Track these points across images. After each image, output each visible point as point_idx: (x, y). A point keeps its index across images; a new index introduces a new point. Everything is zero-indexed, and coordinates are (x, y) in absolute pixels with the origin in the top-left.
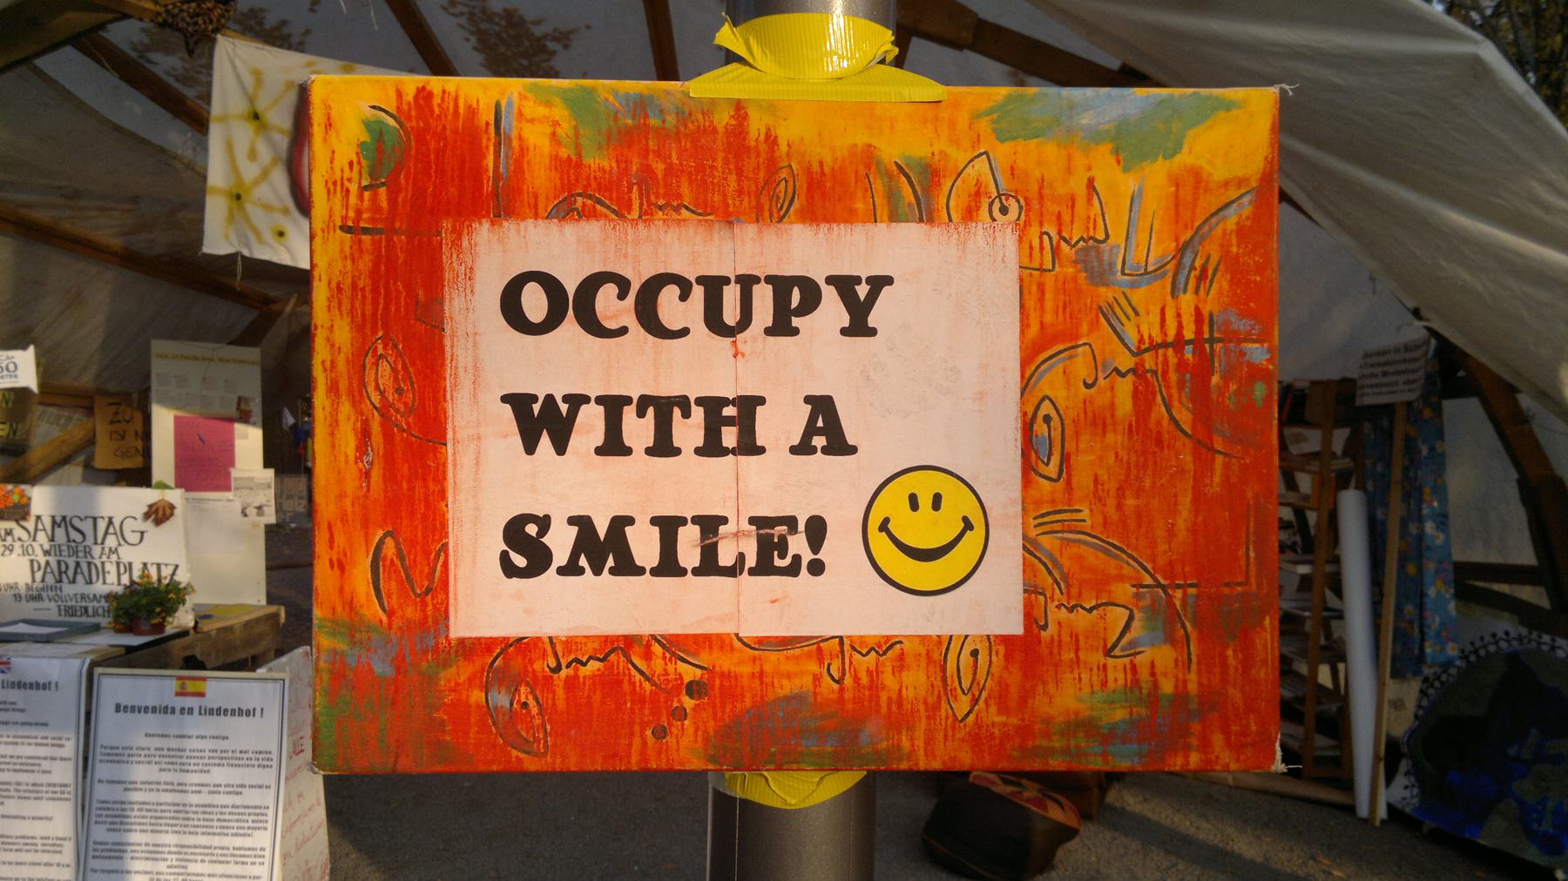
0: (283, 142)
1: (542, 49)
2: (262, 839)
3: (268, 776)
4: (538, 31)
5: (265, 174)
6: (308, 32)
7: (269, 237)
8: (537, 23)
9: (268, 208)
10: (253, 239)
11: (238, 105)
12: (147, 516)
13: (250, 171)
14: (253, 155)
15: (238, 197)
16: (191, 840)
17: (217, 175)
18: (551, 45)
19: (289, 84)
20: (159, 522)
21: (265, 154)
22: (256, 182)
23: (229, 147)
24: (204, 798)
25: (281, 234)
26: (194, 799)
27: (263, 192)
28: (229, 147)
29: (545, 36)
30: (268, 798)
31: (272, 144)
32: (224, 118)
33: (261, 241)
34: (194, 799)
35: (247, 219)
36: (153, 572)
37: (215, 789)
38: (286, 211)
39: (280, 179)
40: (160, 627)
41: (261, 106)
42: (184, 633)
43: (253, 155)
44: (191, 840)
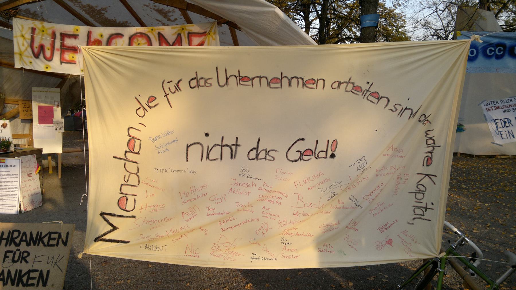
0: (29, 41)
1: (101, 13)
2: (17, 192)
3: (17, 179)
4: (98, 9)
5: (26, 49)
6: (42, 13)
7: (28, 63)
8: (96, 7)
9: (28, 57)
10: (25, 64)
11: (19, 34)
12: (2, 126)
13: (23, 48)
14: (23, 45)
15: (21, 55)
16: (3, 193)
17: (16, 50)
18: (103, 12)
19: (29, 28)
20: (4, 127)
21: (26, 45)
22: (24, 51)
23: (18, 43)
24: (6, 184)
25: (31, 63)
26: (3, 184)
27: (26, 53)
28: (18, 43)
29: (100, 10)
30: (17, 184)
31: (27, 42)
32: (16, 37)
33: (27, 65)
34: (3, 184)
35: (23, 59)
36: (5, 138)
37: (7, 182)
38: (32, 57)
39: (29, 50)
40: (6, 151)
41: (23, 34)
42: (12, 152)
43: (23, 45)
44: (3, 193)
